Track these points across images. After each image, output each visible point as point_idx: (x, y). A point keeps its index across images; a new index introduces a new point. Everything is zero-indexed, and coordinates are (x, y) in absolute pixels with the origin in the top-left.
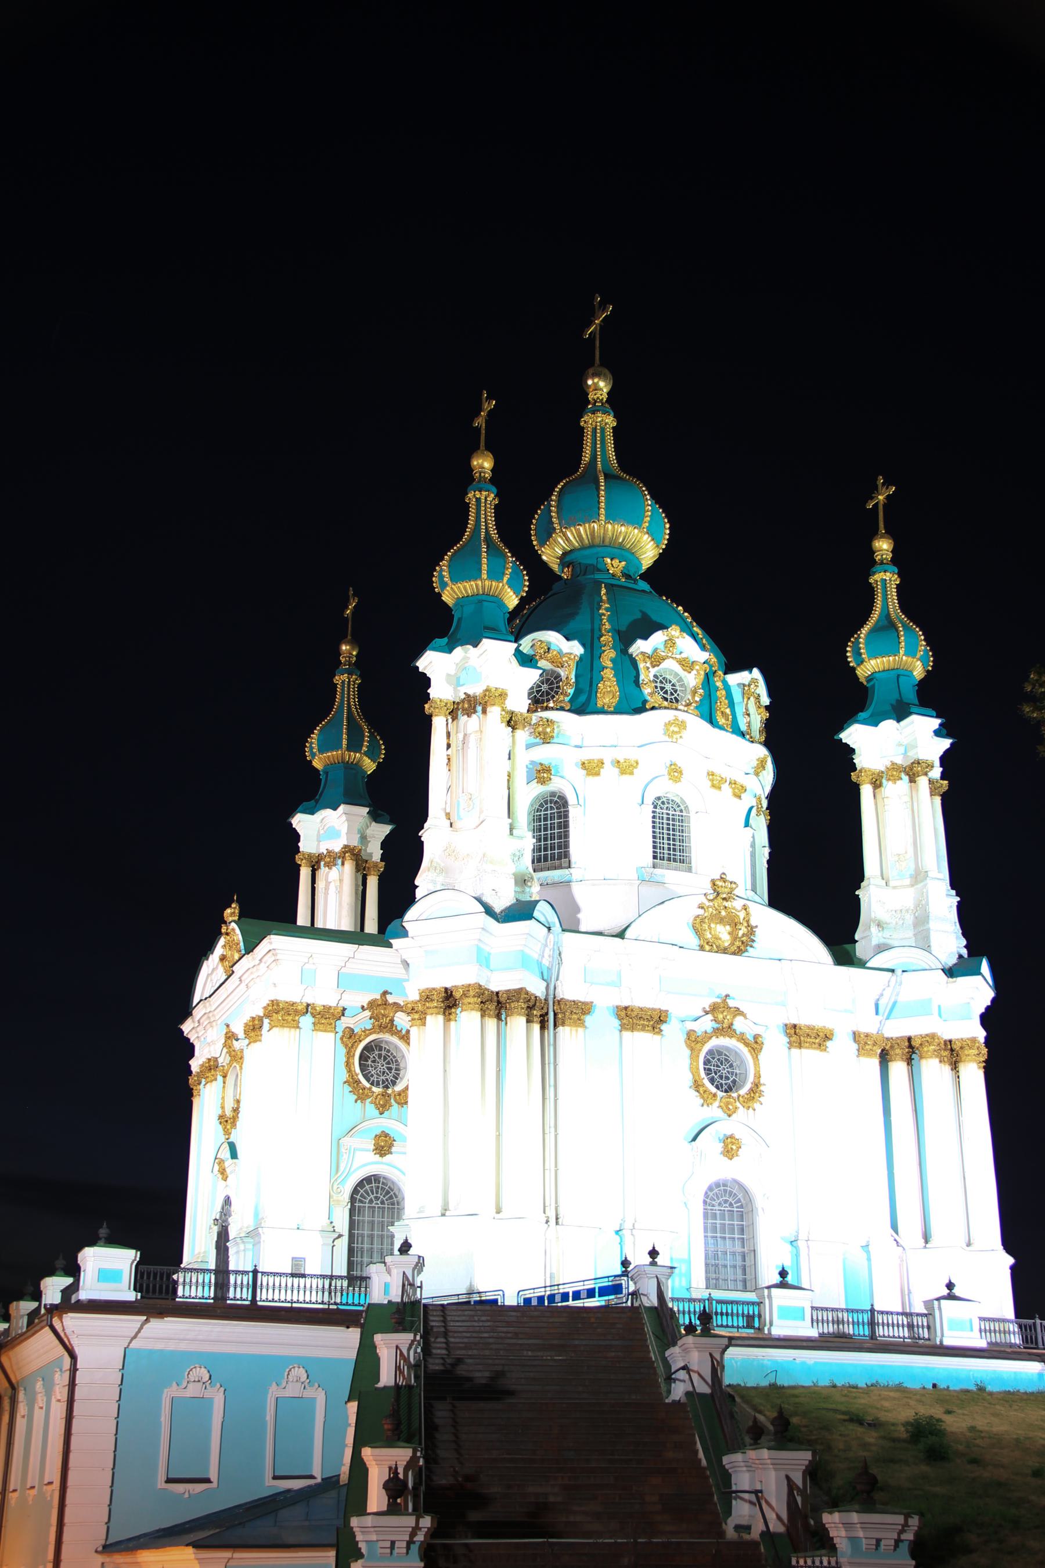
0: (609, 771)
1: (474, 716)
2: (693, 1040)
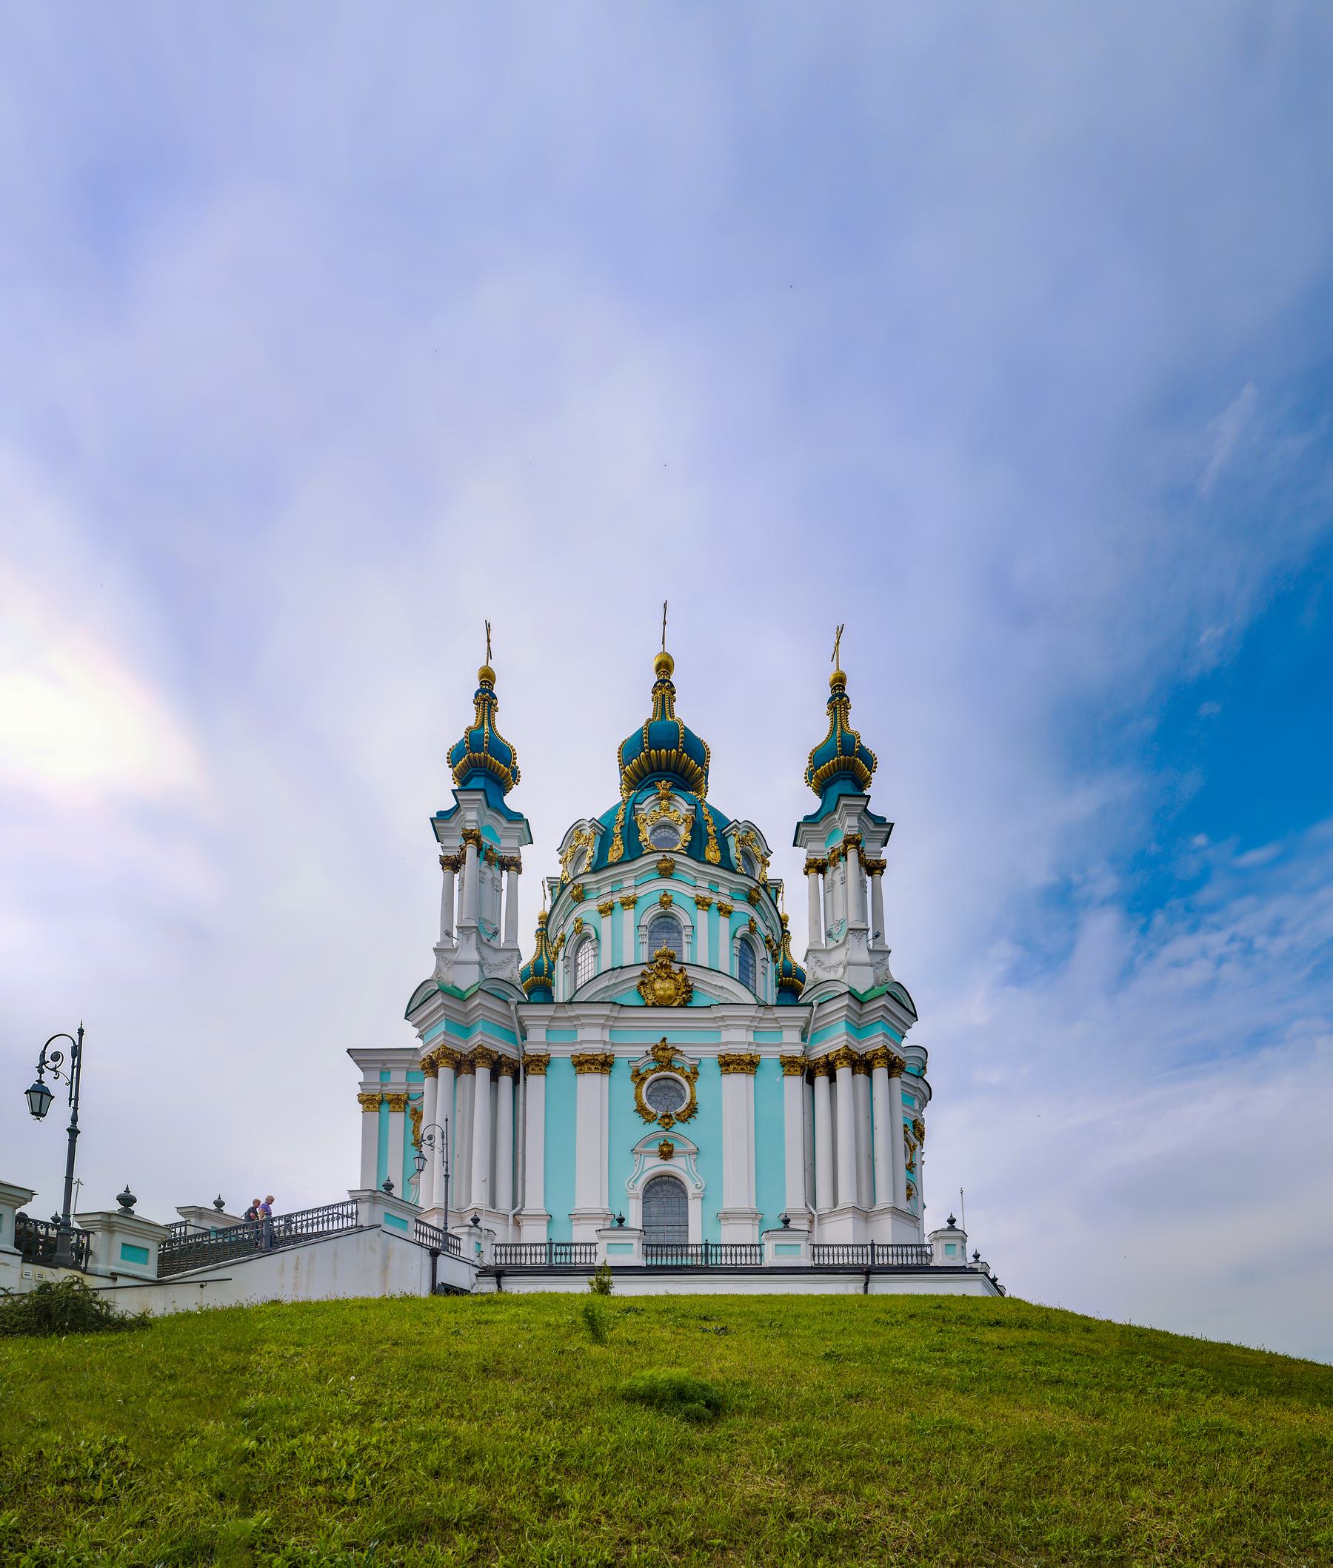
2: (638, 1077)
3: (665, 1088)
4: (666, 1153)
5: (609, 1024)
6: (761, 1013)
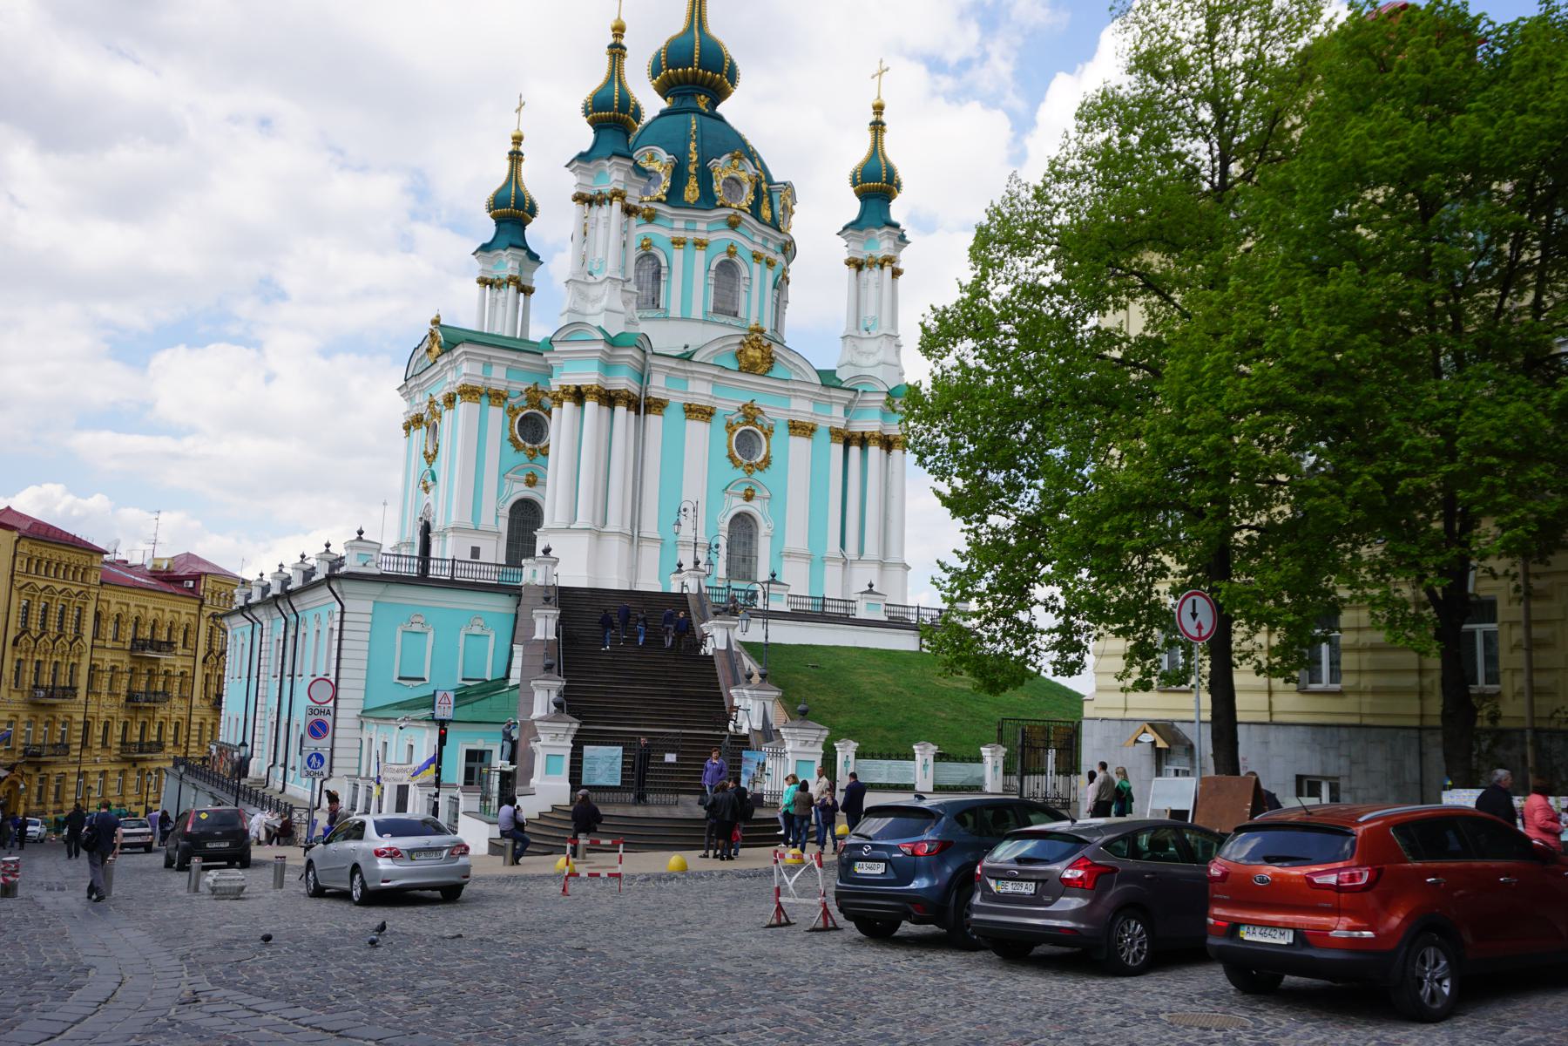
0: (690, 246)
2: (730, 427)
3: (746, 443)
4: (748, 497)
5: (714, 381)
6: (822, 391)
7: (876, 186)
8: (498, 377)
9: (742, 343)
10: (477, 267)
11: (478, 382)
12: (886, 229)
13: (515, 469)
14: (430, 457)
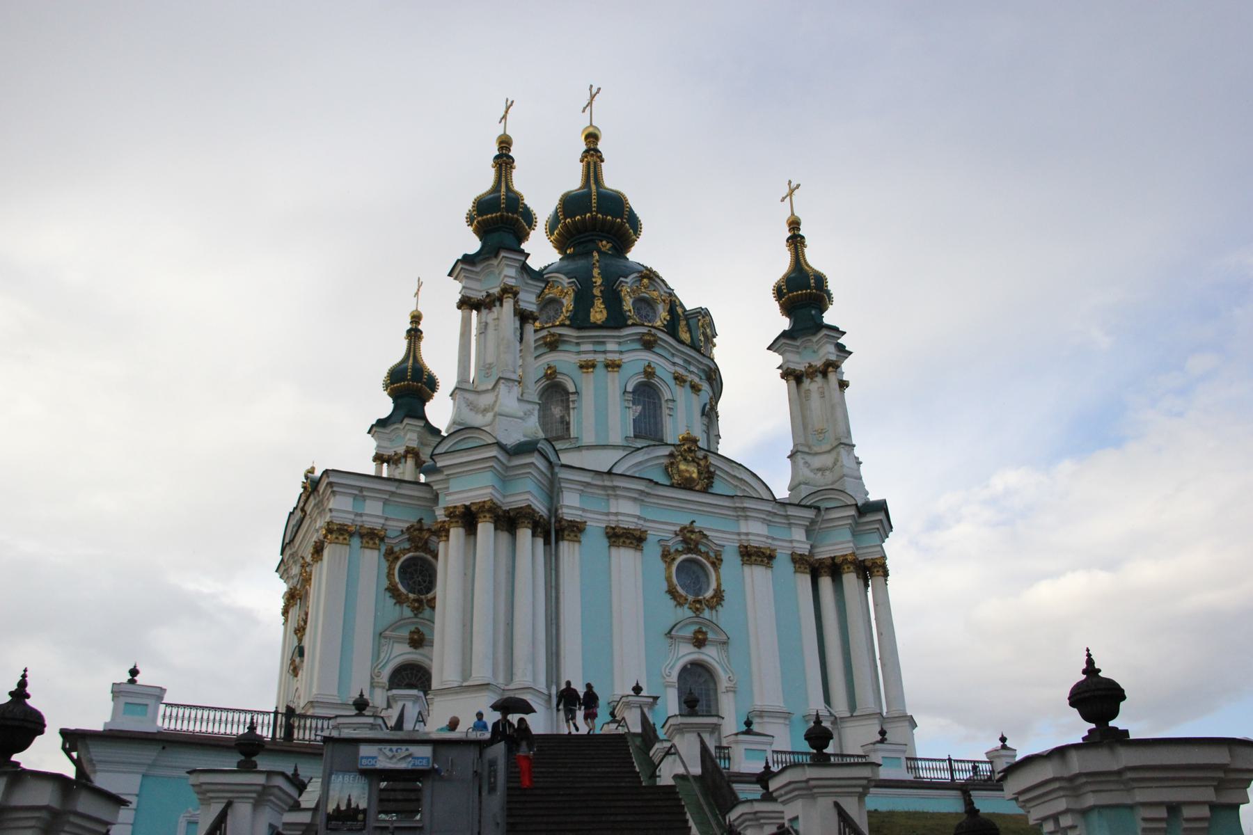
0: (600, 370)
1: (494, 309)
2: (667, 556)
4: (699, 641)
5: (640, 498)
7: (803, 296)
8: (373, 513)
9: (671, 455)
10: (370, 446)
11: (347, 519)
12: (824, 332)
13: (395, 626)
14: (300, 631)
